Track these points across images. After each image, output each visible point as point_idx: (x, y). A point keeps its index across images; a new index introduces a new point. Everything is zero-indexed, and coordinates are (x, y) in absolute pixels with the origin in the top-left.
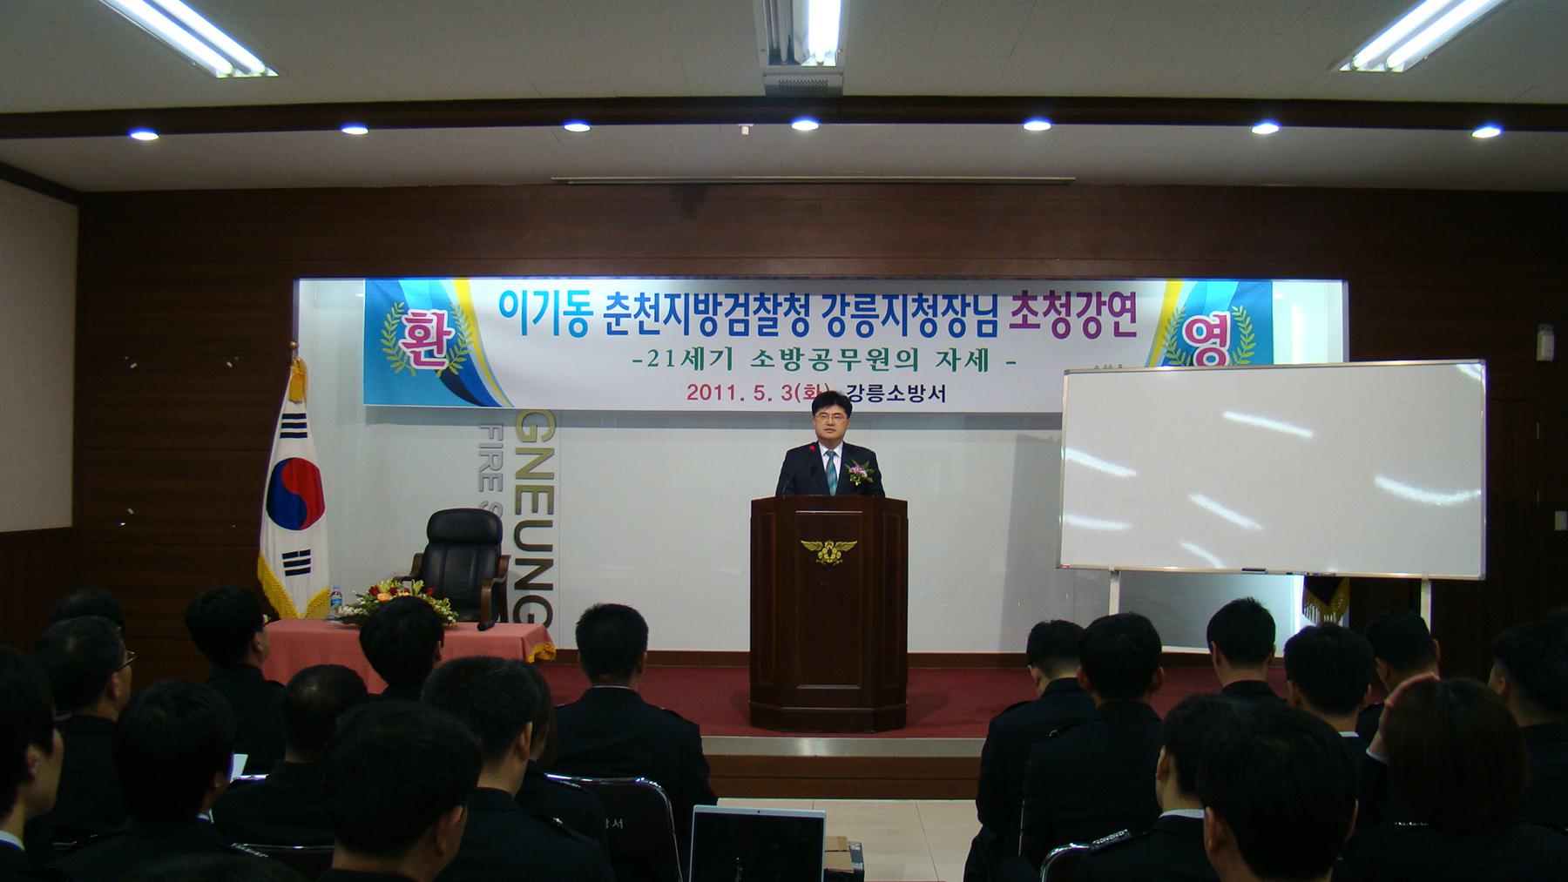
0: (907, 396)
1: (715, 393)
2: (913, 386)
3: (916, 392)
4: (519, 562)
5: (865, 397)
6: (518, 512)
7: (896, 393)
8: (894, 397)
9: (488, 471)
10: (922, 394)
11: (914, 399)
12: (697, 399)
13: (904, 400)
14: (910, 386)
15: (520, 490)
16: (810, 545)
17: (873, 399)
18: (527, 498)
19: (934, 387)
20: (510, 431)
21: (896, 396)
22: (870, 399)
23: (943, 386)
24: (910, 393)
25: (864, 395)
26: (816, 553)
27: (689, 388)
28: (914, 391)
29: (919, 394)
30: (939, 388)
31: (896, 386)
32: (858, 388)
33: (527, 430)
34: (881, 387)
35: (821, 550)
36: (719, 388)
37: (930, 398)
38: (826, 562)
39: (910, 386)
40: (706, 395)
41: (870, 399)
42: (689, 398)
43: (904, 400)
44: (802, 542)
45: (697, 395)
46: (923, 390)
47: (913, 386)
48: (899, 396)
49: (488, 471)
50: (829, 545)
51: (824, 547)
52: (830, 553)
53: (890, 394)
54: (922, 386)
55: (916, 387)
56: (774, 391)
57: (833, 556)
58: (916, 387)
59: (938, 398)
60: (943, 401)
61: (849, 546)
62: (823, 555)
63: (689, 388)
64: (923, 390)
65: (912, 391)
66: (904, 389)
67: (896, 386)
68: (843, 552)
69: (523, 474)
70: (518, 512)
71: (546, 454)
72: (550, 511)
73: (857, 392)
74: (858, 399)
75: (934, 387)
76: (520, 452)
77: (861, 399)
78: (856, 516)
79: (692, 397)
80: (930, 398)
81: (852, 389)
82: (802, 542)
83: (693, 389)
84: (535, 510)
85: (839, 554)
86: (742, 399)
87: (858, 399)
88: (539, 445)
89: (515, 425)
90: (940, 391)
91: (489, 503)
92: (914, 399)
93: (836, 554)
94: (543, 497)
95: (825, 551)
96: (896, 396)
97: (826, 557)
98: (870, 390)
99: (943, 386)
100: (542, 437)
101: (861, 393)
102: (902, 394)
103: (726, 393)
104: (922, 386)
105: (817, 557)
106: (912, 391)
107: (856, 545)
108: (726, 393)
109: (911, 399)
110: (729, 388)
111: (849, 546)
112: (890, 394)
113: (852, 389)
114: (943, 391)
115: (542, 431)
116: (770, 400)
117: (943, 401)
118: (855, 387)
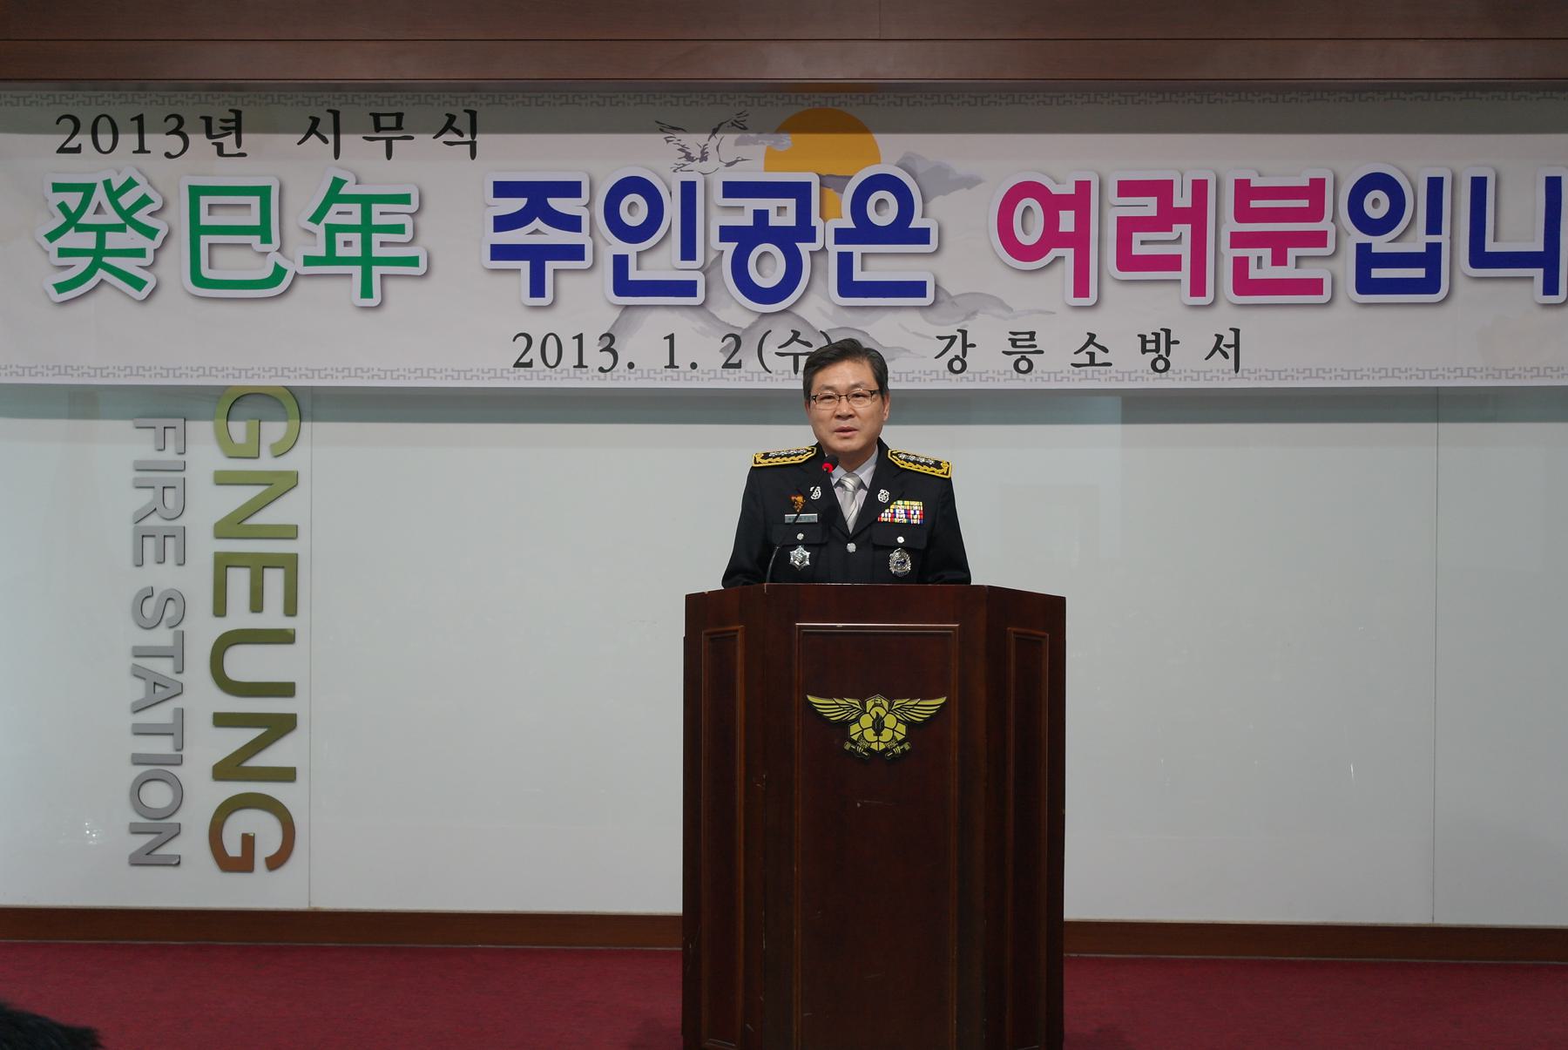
4: (223, 720)
6: (220, 609)
9: (154, 521)
15: (224, 563)
16: (829, 707)
18: (239, 580)
20: (202, 432)
26: (844, 725)
33: (238, 429)
35: (857, 720)
38: (869, 750)
44: (811, 698)
49: (154, 521)
50: (876, 706)
51: (866, 713)
52: (878, 726)
57: (887, 735)
62: (862, 729)
69: (231, 526)
70: (220, 609)
71: (280, 485)
72: (291, 608)
76: (223, 479)
78: (942, 637)
82: (811, 698)
84: (257, 605)
85: (902, 728)
88: (266, 463)
89: (211, 418)
91: (156, 595)
93: (894, 729)
94: (274, 580)
95: (866, 721)
97: (870, 735)
100: (272, 446)
115: (274, 431)
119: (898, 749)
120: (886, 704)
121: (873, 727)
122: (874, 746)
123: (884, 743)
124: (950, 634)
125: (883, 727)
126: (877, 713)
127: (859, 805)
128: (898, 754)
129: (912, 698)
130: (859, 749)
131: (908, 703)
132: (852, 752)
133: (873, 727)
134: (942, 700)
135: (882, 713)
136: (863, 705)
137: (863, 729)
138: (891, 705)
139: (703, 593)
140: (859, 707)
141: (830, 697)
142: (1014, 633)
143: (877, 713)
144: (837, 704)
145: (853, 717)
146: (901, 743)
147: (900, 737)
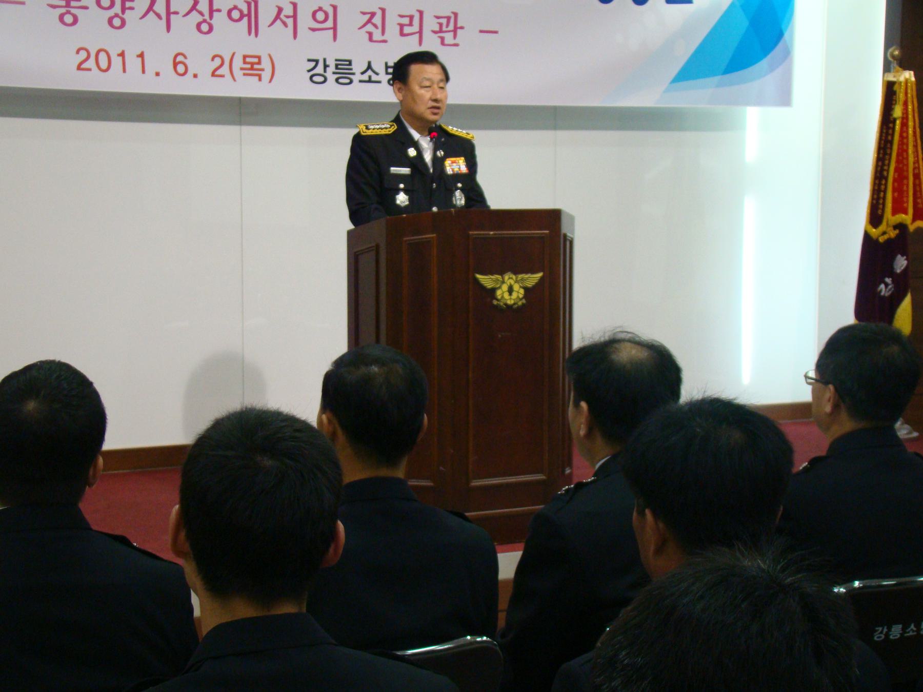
1: (117, 62)
5: (331, 78)
7: (370, 73)
8: (367, 79)
12: (89, 70)
13: (379, 82)
14: (386, 64)
16: (486, 280)
17: (341, 81)
21: (370, 77)
26: (493, 290)
27: (78, 52)
31: (369, 63)
34: (350, 63)
35: (500, 288)
36: (122, 55)
38: (506, 304)
39: (386, 64)
40: (104, 64)
41: (337, 80)
42: (79, 68)
43: (379, 82)
44: (478, 276)
45: (91, 63)
48: (374, 78)
50: (510, 279)
51: (503, 282)
52: (510, 290)
53: (363, 73)
56: (200, 63)
57: (514, 295)
61: (533, 279)
62: (502, 292)
66: (379, 67)
67: (369, 63)
73: (320, 69)
74: (321, 79)
77: (325, 80)
79: (83, 66)
81: (313, 64)
82: (478, 276)
85: (522, 291)
86: (157, 74)
87: (321, 79)
93: (518, 292)
95: (505, 288)
96: (370, 77)
97: (506, 296)
98: (337, 66)
101: (325, 71)
102: (377, 74)
103: (133, 63)
108: (133, 63)
110: (138, 56)
111: (533, 279)
112: (363, 73)
113: (313, 64)
118: (317, 62)
119: (520, 303)
120: (514, 277)
122: (509, 302)
130: (502, 304)
132: (496, 307)
134: (540, 275)
135: (512, 282)
136: (503, 278)
137: (503, 293)
138: (516, 278)
144: (491, 278)
145: (498, 286)
146: (521, 299)
147: (521, 296)
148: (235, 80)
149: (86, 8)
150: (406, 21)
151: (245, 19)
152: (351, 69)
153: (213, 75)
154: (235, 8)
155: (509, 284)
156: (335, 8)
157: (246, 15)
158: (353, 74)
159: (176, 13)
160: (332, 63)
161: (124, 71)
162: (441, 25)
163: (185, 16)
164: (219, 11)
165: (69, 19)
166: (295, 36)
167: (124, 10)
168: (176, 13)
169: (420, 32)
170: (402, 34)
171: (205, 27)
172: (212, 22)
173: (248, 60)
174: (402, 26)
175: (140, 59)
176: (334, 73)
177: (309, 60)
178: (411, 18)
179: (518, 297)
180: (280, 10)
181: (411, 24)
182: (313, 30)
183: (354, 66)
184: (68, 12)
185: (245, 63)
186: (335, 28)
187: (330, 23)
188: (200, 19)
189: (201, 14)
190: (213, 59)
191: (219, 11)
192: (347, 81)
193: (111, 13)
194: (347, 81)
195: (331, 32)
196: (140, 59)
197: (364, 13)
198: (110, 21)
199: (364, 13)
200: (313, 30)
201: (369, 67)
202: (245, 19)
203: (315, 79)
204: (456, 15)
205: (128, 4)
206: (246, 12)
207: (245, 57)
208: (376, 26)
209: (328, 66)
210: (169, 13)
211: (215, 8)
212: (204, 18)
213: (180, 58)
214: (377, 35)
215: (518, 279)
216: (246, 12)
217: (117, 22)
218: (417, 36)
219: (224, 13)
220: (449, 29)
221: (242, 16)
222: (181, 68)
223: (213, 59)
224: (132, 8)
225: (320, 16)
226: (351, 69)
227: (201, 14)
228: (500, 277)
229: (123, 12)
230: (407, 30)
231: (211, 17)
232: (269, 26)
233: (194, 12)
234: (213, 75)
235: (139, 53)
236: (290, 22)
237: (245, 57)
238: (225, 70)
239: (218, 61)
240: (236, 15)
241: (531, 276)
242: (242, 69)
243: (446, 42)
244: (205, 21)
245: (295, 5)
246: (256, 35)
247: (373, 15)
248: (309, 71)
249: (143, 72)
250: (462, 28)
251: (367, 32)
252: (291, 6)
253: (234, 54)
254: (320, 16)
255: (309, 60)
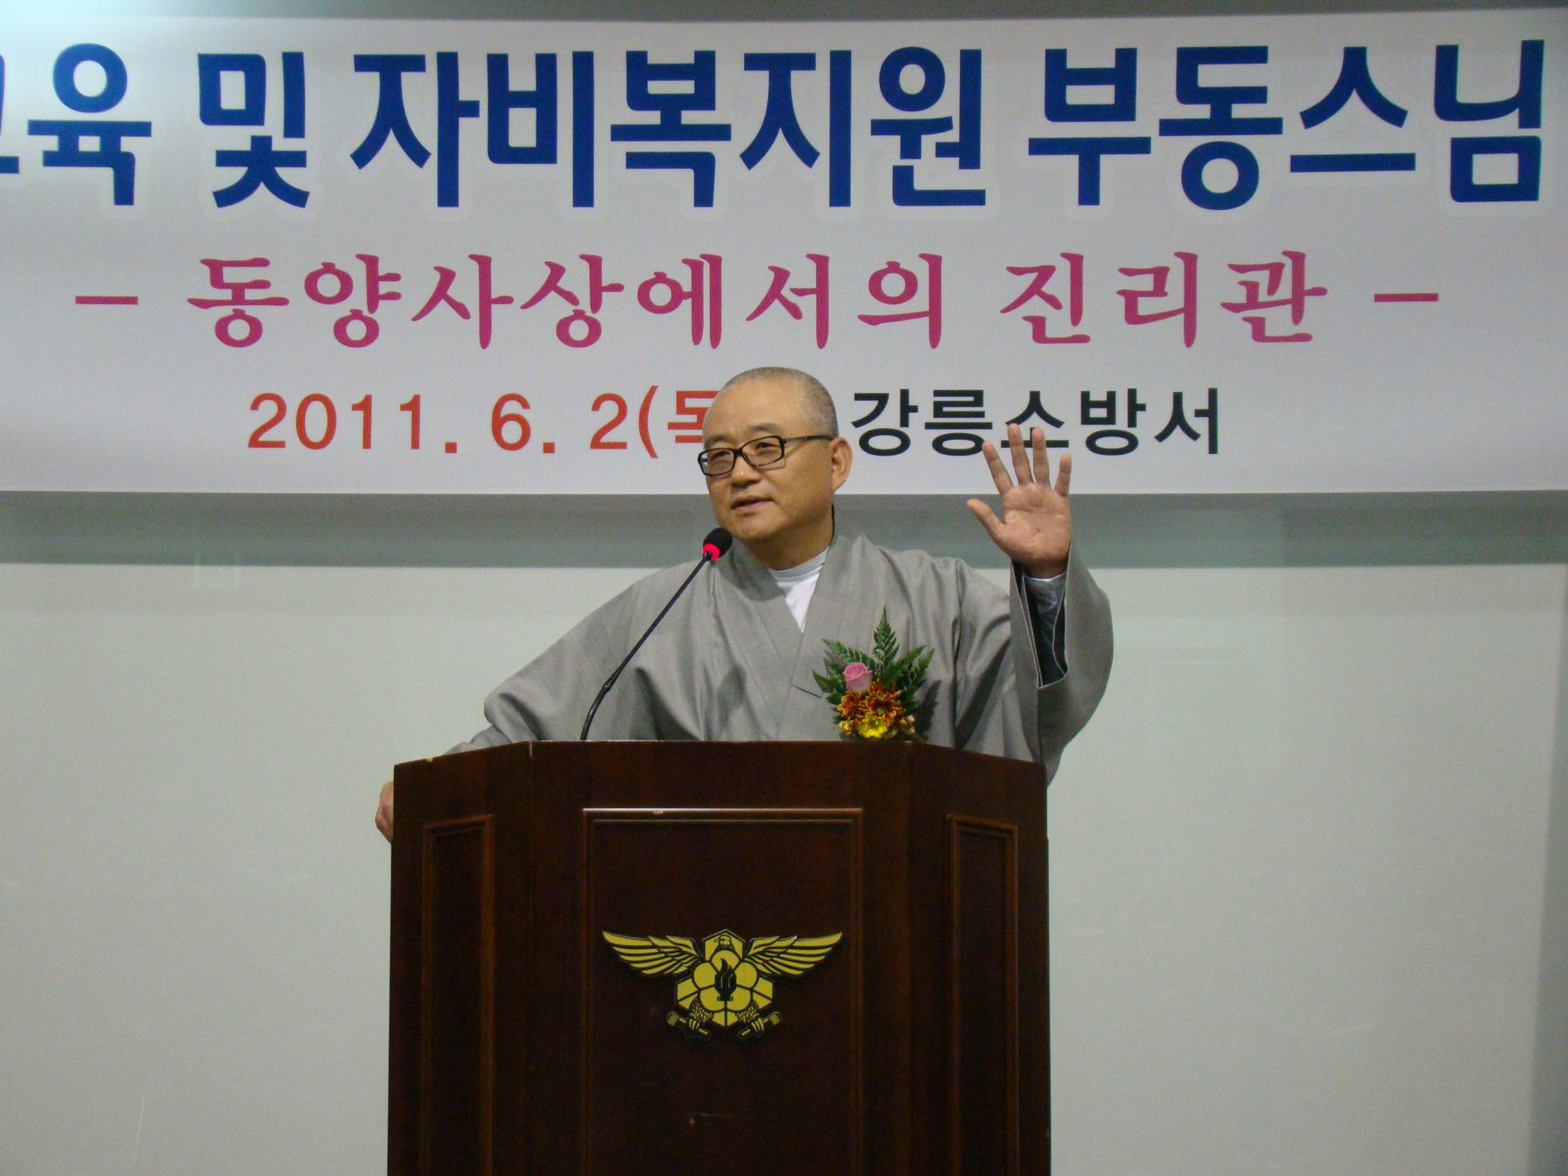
0: (1076, 433)
1: (350, 423)
2: (1098, 395)
3: (1111, 419)
7: (1035, 419)
10: (1132, 422)
11: (1102, 443)
12: (281, 444)
14: (1085, 395)
17: (948, 444)
19: (1178, 398)
22: (938, 445)
23: (1213, 394)
24: (1086, 420)
25: (917, 429)
26: (667, 983)
27: (255, 406)
28: (1101, 413)
29: (1121, 423)
30: (1195, 401)
31: (1035, 397)
32: (893, 406)
34: (978, 397)
35: (689, 974)
36: (365, 406)
37: (1161, 437)
38: (710, 1025)
39: (1085, 395)
40: (316, 431)
42: (255, 442)
44: (610, 938)
45: (286, 430)
46: (1134, 407)
47: (1098, 395)
50: (722, 949)
51: (703, 960)
52: (726, 983)
54: (1132, 394)
55: (1111, 396)
57: (740, 999)
58: (1111, 396)
59: (1194, 436)
60: (1213, 448)
63: (255, 406)
64: (1134, 407)
65: (1095, 413)
67: (1035, 397)
68: (780, 980)
74: (894, 442)
75: (1178, 398)
77: (905, 443)
79: (264, 438)
80: (1161, 437)
81: (873, 405)
82: (610, 938)
83: (270, 408)
85: (766, 987)
86: (451, 448)
87: (894, 442)
90: (1199, 413)
92: (1101, 443)
95: (705, 975)
97: (711, 999)
98: (938, 409)
99: (1213, 394)
101: (904, 422)
103: (391, 423)
104: (1132, 394)
105: (672, 1004)
106: (1095, 413)
107: (836, 947)
108: (391, 423)
109: (1091, 443)
110: (404, 408)
113: (873, 405)
114: (1211, 413)
116: (549, 448)
117: (1213, 448)
118: (882, 399)
119: (760, 1024)
120: (738, 945)
121: (717, 986)
122: (719, 1019)
123: (736, 1012)
124: (847, 825)
125: (734, 986)
126: (724, 962)
127: (692, 1122)
128: (759, 1032)
129: (784, 936)
130: (693, 1024)
131: (777, 944)
133: (717, 986)
134: (834, 939)
135: (732, 960)
136: (700, 948)
137: (699, 990)
138: (747, 947)
139: (424, 762)
140: (693, 952)
141: (643, 936)
142: (960, 823)
143: (724, 962)
144: (654, 946)
145: (683, 969)
146: (764, 1012)
147: (762, 1003)
148: (653, 454)
149: (281, 302)
150: (1146, 283)
151: (687, 304)
152: (981, 415)
153: (597, 443)
154: (660, 278)
155: (719, 966)
156: (934, 262)
157: (686, 296)
158: (988, 426)
159: (506, 300)
160: (924, 402)
161: (367, 444)
162: (1252, 288)
163: (525, 306)
164: (617, 288)
165: (239, 330)
166: (822, 338)
167: (373, 300)
168: (506, 300)
169: (1189, 310)
170: (1133, 317)
171: (579, 330)
172: (596, 316)
173: (690, 403)
174: (1131, 298)
175: (408, 414)
176: (929, 426)
177: (859, 397)
178: (1160, 274)
179: (752, 1003)
180: (781, 276)
181: (1159, 290)
182: (873, 320)
183: (985, 408)
184: (239, 315)
185: (681, 409)
186: (934, 314)
187: (921, 301)
188: (567, 310)
189: (571, 298)
190: (596, 406)
191: (617, 288)
192: (970, 444)
193: (343, 309)
194: (970, 444)
195: (926, 321)
196: (408, 414)
197: (1018, 271)
198: (340, 329)
199: (1018, 271)
200: (873, 320)
201: (1035, 405)
202: (687, 304)
203: (875, 442)
204: (1298, 259)
205: (384, 287)
206: (687, 286)
207: (682, 396)
208: (1054, 302)
209: (915, 409)
210: (486, 301)
211: (605, 282)
212: (578, 308)
213: (511, 408)
214: (1059, 322)
215: (750, 953)
216: (687, 286)
217: (356, 330)
218: (1180, 319)
219: (631, 291)
220: (1278, 296)
221: (678, 296)
222: (511, 432)
223: (596, 406)
224: (394, 296)
225: (893, 285)
226: (981, 415)
227: (571, 298)
228: (689, 943)
229: (373, 306)
230: (1145, 306)
231: (596, 304)
232: (750, 318)
233: (553, 295)
234: (597, 443)
235: (407, 399)
236: (808, 305)
237: (682, 396)
238: (627, 431)
239: (610, 410)
240: (660, 295)
241: (796, 944)
242: (672, 426)
243: (1269, 332)
244: (579, 315)
245: (821, 263)
246: (715, 341)
247: (1045, 272)
248: (857, 424)
249: (415, 444)
250: (1320, 292)
251: (1027, 318)
252: (813, 265)
253: (653, 390)
254: (893, 285)
255: (859, 397)
